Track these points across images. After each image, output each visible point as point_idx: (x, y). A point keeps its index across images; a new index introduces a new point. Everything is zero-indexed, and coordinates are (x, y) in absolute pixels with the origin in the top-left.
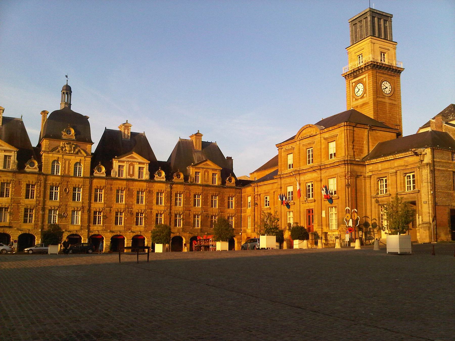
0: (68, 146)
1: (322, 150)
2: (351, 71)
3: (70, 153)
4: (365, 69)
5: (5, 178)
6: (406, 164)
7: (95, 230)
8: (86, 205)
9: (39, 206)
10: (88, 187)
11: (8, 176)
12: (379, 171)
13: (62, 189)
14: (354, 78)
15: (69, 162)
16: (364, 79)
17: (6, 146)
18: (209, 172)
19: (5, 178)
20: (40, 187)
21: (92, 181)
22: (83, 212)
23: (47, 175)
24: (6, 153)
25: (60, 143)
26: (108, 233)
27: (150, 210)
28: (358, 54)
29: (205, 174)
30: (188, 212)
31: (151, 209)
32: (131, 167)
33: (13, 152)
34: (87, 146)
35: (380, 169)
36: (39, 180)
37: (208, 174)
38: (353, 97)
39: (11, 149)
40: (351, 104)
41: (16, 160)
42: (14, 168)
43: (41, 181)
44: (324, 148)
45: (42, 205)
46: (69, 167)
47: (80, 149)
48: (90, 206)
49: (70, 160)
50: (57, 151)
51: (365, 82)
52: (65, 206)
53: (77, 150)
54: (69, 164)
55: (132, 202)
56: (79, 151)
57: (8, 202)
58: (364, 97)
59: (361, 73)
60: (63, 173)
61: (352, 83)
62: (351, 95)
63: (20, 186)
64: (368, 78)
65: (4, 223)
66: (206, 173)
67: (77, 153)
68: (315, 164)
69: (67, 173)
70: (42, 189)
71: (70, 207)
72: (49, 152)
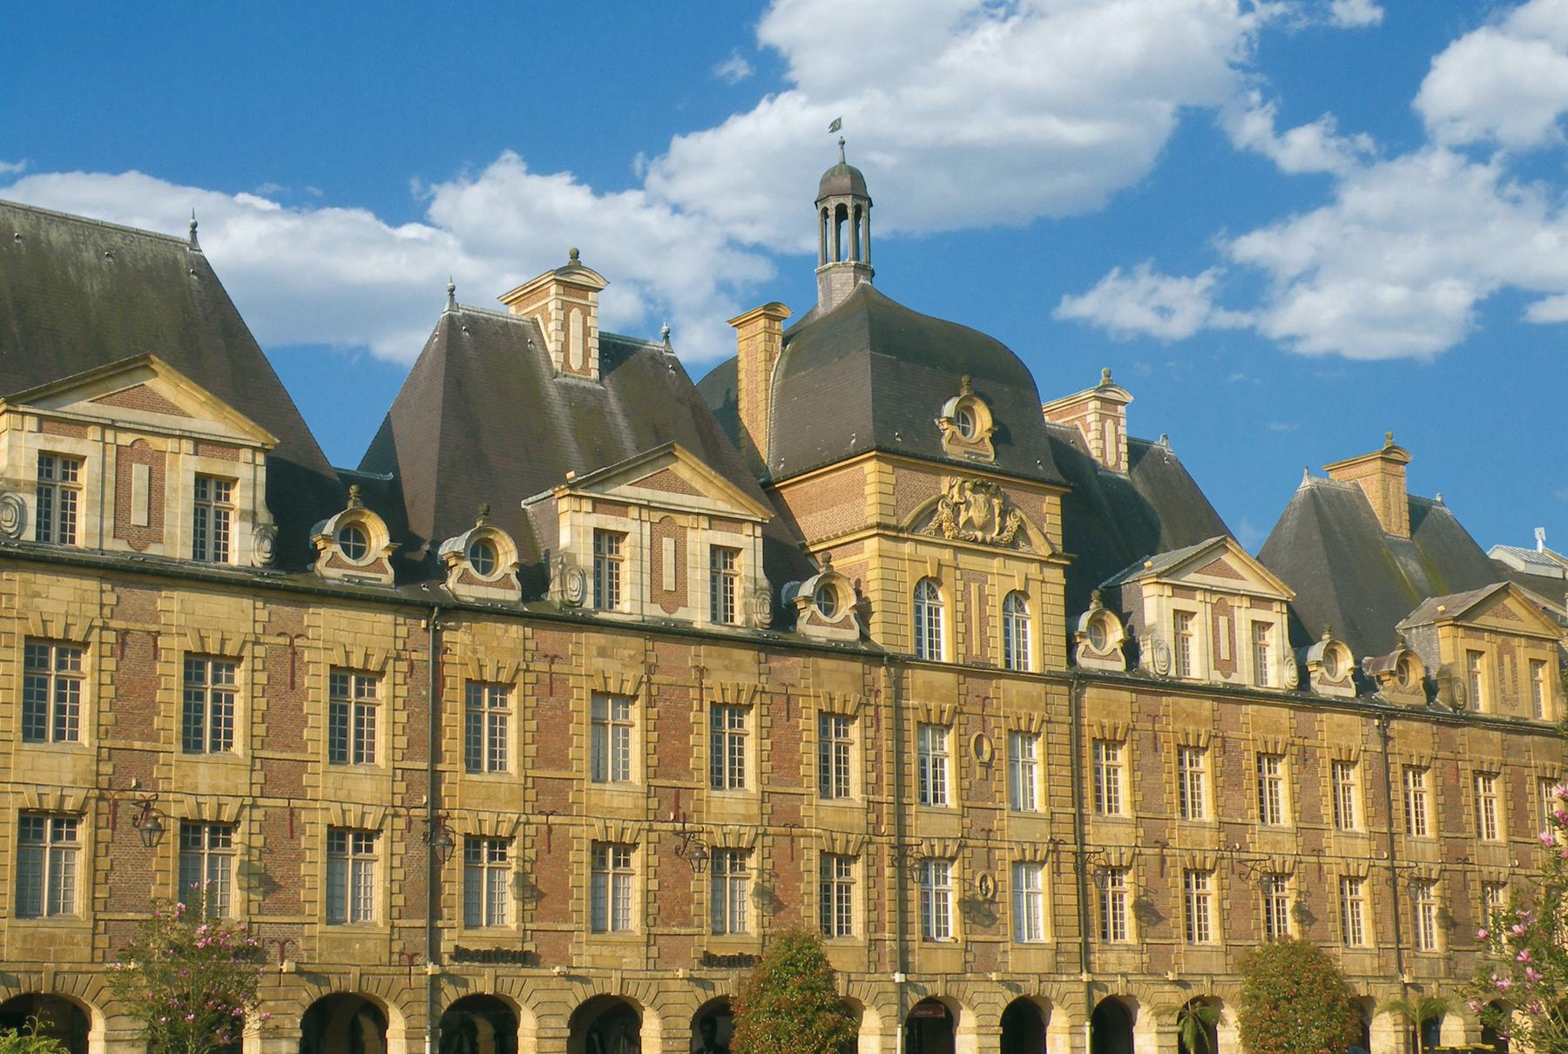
0: (981, 497)
3: (988, 539)
5: (728, 679)
7: (1110, 969)
8: (1066, 832)
9: (878, 839)
10: (1066, 728)
11: (739, 667)
13: (964, 740)
15: (981, 590)
17: (714, 492)
18: (1517, 652)
19: (728, 679)
20: (878, 730)
21: (1079, 697)
22: (1056, 872)
23: (898, 663)
24: (719, 534)
25: (938, 483)
26: (1167, 988)
27: (1314, 859)
29: (1501, 663)
30: (1459, 867)
31: (1319, 852)
32: (1223, 621)
33: (748, 529)
34: (1044, 502)
36: (871, 690)
37: (1514, 665)
39: (738, 512)
41: (760, 573)
42: (756, 618)
43: (876, 696)
45: (893, 830)
46: (983, 620)
47: (1024, 517)
48: (1080, 839)
49: (981, 577)
50: (933, 525)
52: (984, 835)
53: (1012, 523)
54: (983, 599)
55: (1241, 816)
56: (1021, 529)
57: (747, 817)
60: (962, 649)
63: (792, 722)
65: (735, 939)
66: (1507, 658)
67: (1013, 544)
69: (975, 651)
70: (887, 744)
71: (1006, 845)
72: (901, 530)
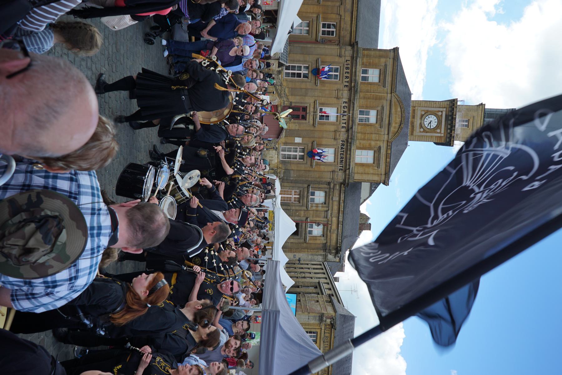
1: (369, 142)
2: (456, 115)
4: (449, 133)
6: (332, 231)
12: (332, 197)
14: (446, 115)
16: (438, 131)
28: (471, 121)
35: (334, 199)
38: (427, 111)
40: (419, 108)
44: (370, 144)
51: (436, 131)
58: (420, 128)
59: (448, 126)
61: (442, 112)
62: (430, 109)
64: (438, 137)
68: (356, 127)
